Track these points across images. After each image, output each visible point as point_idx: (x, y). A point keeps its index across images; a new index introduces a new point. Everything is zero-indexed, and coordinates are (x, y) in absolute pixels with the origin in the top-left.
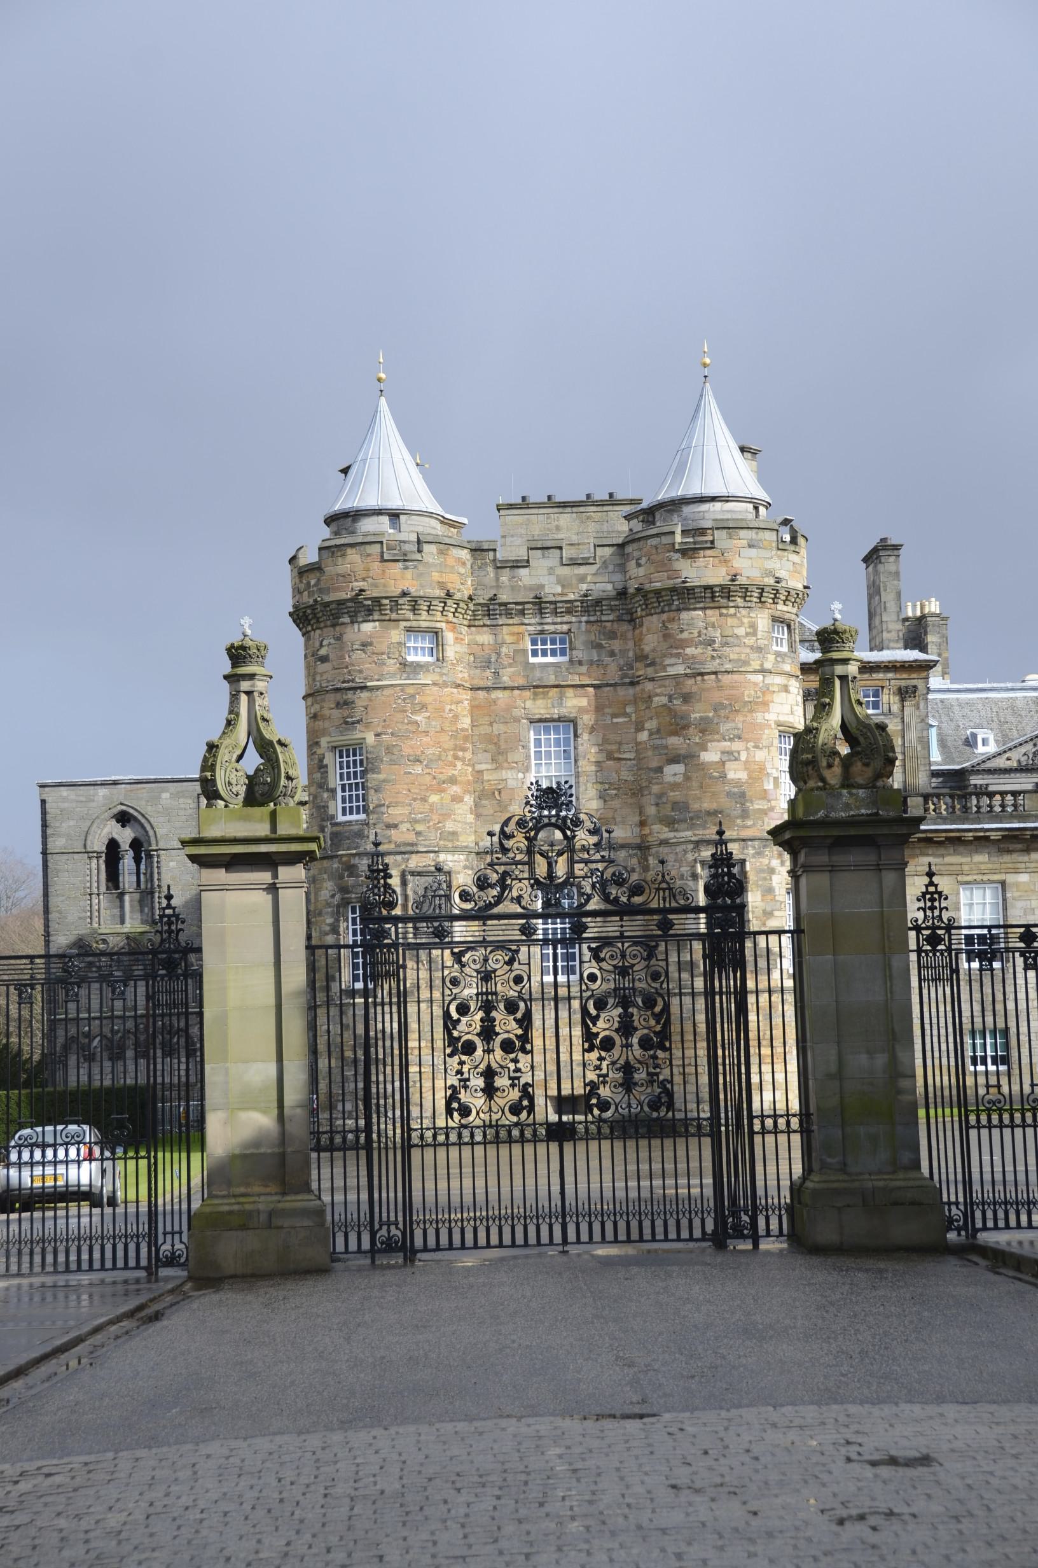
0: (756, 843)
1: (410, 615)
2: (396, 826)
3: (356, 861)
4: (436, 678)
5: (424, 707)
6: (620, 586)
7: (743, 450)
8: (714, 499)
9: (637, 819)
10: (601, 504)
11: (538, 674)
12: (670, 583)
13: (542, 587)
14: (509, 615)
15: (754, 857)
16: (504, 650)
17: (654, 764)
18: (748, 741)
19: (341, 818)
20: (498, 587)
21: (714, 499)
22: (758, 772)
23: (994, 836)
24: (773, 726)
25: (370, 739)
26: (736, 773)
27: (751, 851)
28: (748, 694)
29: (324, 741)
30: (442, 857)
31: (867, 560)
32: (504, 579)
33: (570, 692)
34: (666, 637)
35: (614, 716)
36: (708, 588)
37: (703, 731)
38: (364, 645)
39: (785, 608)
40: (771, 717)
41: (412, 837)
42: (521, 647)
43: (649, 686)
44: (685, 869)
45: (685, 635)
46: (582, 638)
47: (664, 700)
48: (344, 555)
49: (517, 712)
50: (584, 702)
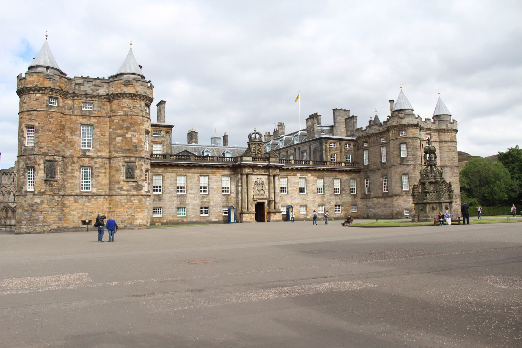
1: (51, 93)
2: (42, 148)
3: (30, 156)
4: (56, 110)
5: (52, 117)
6: (107, 93)
7: (140, 66)
8: (132, 74)
9: (108, 151)
10: (101, 79)
11: (84, 112)
12: (121, 92)
13: (86, 91)
14: (78, 97)
16: (75, 106)
17: (114, 137)
19: (27, 145)
20: (75, 89)
21: (132, 74)
22: (140, 141)
23: (185, 165)
25: (37, 124)
26: (135, 140)
28: (139, 121)
29: (23, 125)
30: (55, 157)
31: (157, 105)
32: (77, 88)
33: (92, 118)
34: (119, 105)
35: (104, 125)
36: (130, 94)
37: (127, 129)
38: (37, 99)
41: (47, 151)
42: (80, 105)
43: (113, 118)
44: (121, 164)
45: (123, 105)
47: (117, 121)
48: (33, 75)
49: (78, 122)
50: (96, 121)
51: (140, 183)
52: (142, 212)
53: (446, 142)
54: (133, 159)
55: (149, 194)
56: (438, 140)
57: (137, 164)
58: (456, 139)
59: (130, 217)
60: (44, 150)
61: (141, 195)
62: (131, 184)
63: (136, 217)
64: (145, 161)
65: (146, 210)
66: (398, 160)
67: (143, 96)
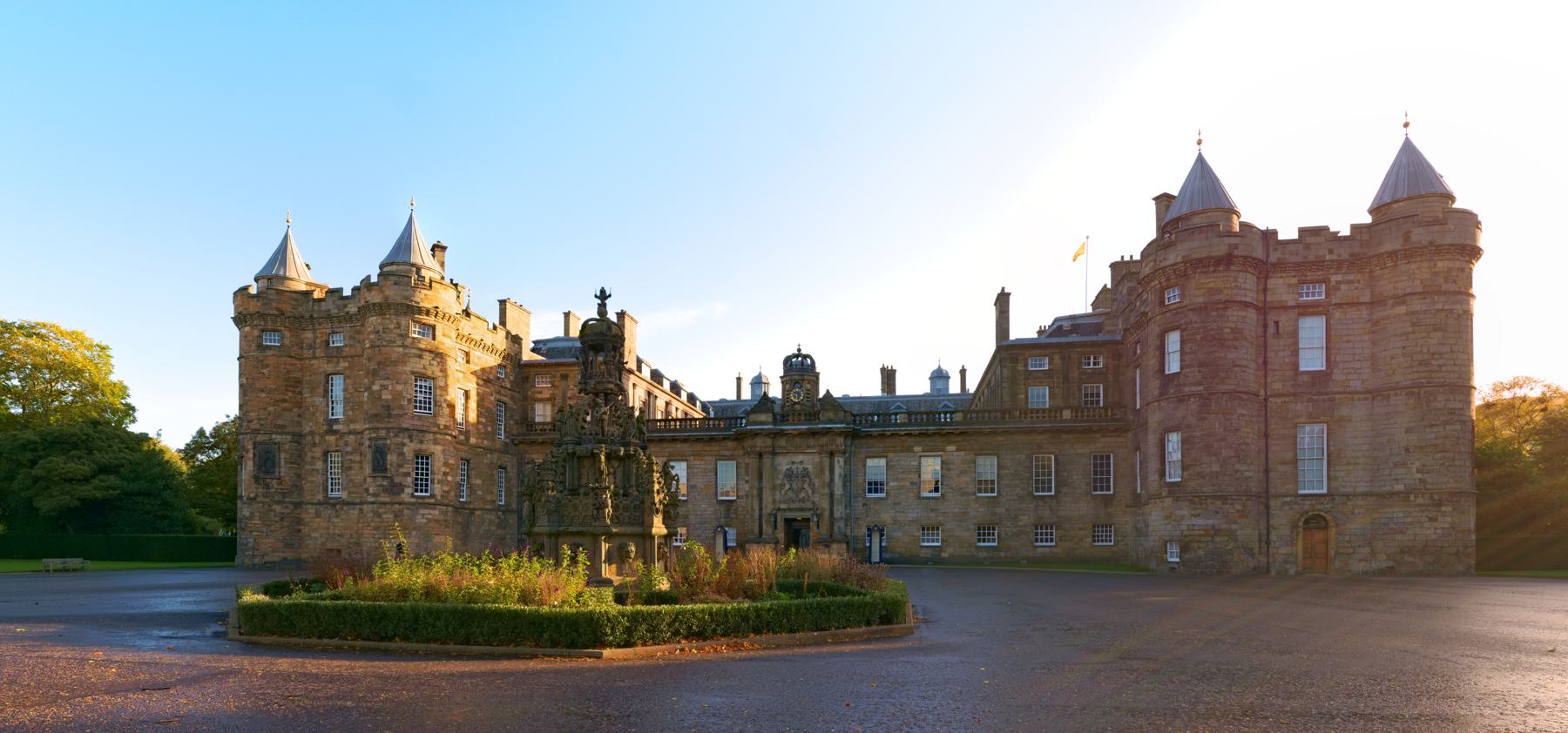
51: (397, 480)
53: (1401, 299)
54: (383, 433)
56: (1366, 298)
58: (1470, 285)
60: (254, 425)
62: (379, 481)
64: (410, 437)
66: (1155, 384)
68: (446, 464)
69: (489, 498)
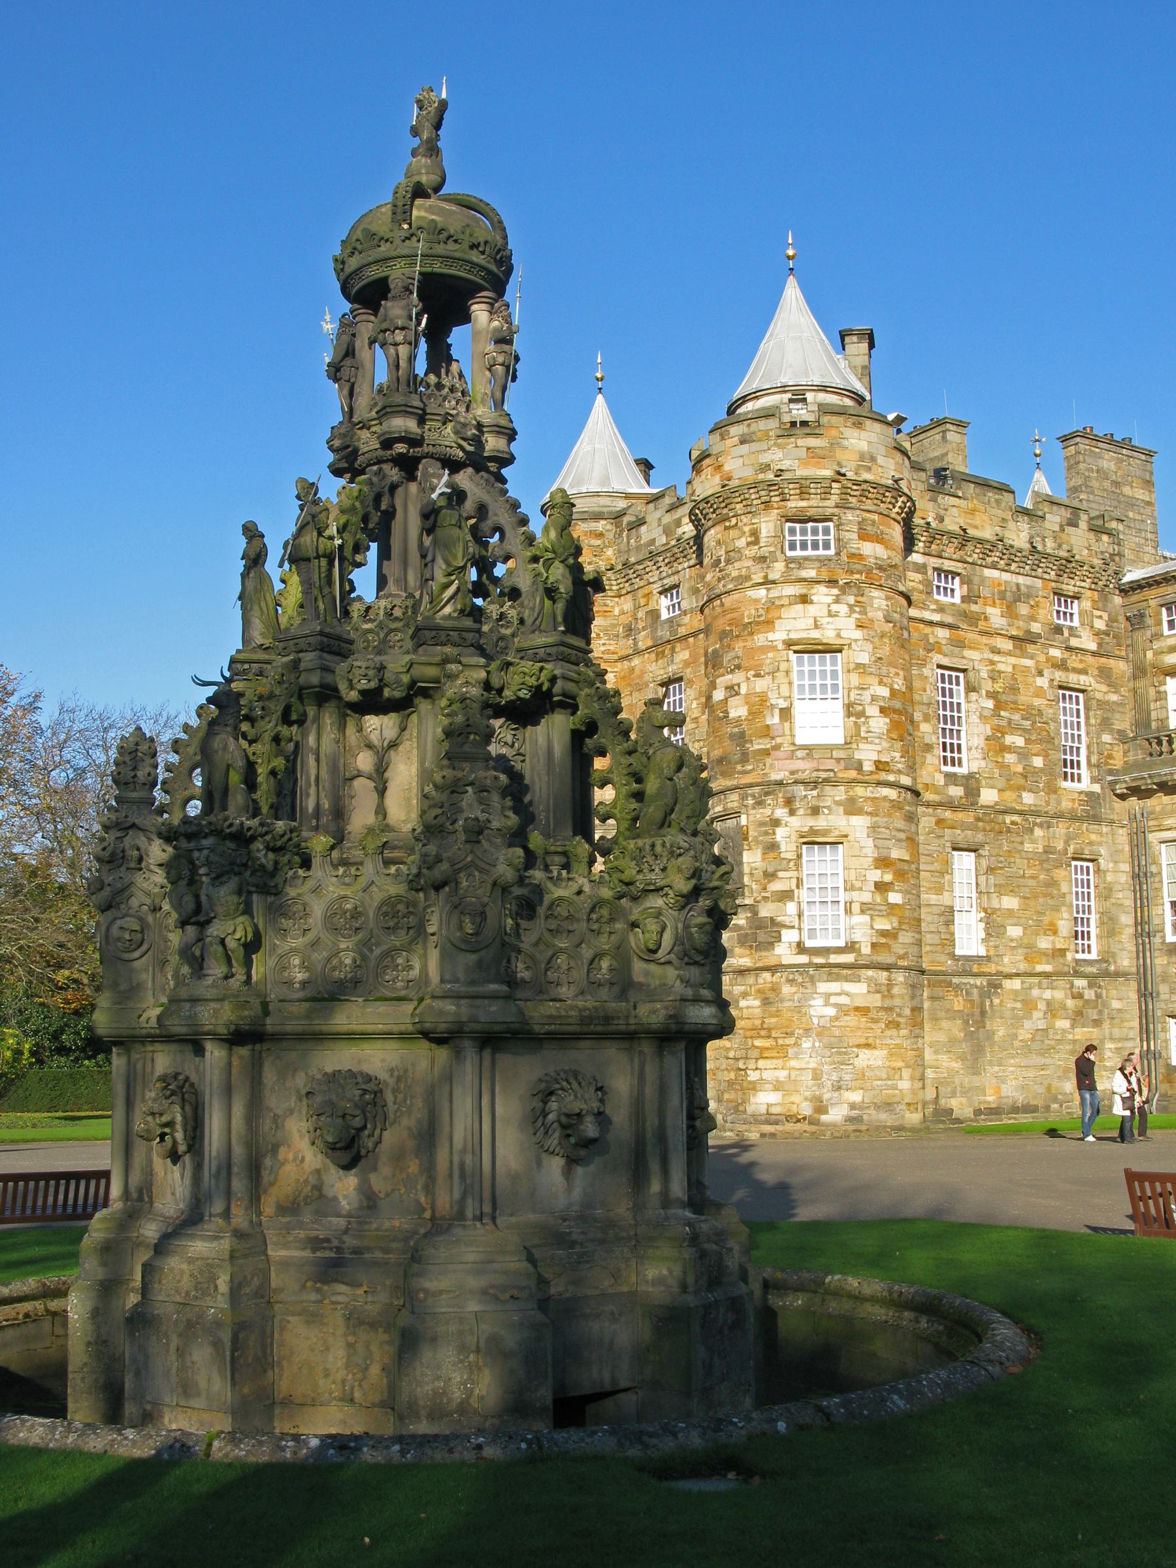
0: (757, 790)
13: (653, 541)
15: (754, 808)
18: (747, 670)
22: (759, 705)
24: (780, 646)
27: (750, 801)
39: (804, 504)
40: (778, 635)
46: (687, 586)
51: (765, 911)
52: (782, 1052)
55: (849, 958)
57: (744, 820)
59: (732, 1075)
61: (772, 969)
63: (753, 1076)
65: (806, 1044)
67: (754, 485)
68: (882, 862)
69: (1044, 943)
